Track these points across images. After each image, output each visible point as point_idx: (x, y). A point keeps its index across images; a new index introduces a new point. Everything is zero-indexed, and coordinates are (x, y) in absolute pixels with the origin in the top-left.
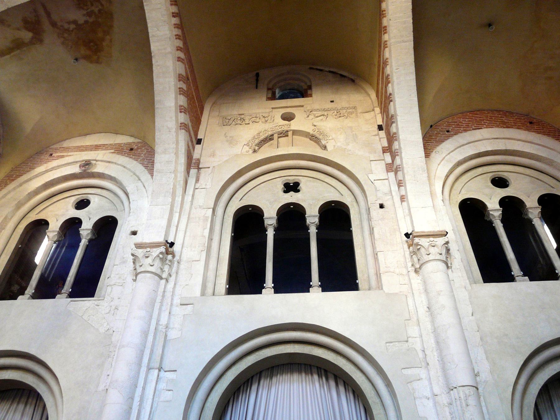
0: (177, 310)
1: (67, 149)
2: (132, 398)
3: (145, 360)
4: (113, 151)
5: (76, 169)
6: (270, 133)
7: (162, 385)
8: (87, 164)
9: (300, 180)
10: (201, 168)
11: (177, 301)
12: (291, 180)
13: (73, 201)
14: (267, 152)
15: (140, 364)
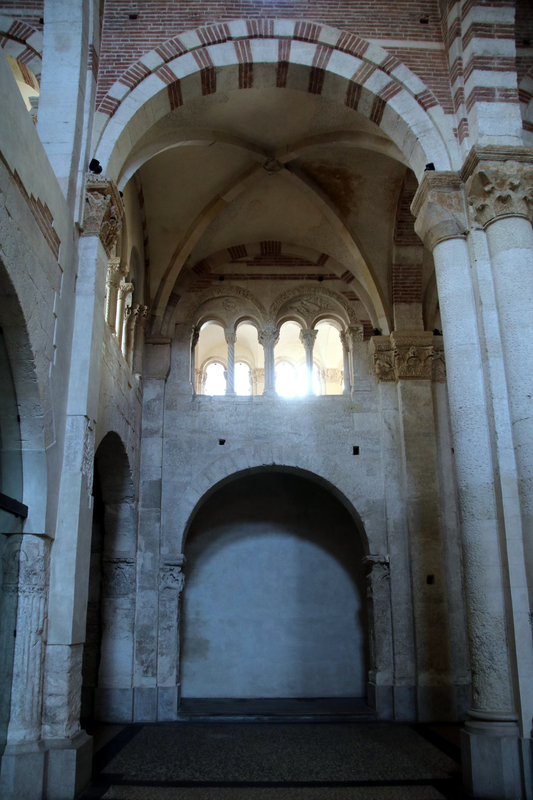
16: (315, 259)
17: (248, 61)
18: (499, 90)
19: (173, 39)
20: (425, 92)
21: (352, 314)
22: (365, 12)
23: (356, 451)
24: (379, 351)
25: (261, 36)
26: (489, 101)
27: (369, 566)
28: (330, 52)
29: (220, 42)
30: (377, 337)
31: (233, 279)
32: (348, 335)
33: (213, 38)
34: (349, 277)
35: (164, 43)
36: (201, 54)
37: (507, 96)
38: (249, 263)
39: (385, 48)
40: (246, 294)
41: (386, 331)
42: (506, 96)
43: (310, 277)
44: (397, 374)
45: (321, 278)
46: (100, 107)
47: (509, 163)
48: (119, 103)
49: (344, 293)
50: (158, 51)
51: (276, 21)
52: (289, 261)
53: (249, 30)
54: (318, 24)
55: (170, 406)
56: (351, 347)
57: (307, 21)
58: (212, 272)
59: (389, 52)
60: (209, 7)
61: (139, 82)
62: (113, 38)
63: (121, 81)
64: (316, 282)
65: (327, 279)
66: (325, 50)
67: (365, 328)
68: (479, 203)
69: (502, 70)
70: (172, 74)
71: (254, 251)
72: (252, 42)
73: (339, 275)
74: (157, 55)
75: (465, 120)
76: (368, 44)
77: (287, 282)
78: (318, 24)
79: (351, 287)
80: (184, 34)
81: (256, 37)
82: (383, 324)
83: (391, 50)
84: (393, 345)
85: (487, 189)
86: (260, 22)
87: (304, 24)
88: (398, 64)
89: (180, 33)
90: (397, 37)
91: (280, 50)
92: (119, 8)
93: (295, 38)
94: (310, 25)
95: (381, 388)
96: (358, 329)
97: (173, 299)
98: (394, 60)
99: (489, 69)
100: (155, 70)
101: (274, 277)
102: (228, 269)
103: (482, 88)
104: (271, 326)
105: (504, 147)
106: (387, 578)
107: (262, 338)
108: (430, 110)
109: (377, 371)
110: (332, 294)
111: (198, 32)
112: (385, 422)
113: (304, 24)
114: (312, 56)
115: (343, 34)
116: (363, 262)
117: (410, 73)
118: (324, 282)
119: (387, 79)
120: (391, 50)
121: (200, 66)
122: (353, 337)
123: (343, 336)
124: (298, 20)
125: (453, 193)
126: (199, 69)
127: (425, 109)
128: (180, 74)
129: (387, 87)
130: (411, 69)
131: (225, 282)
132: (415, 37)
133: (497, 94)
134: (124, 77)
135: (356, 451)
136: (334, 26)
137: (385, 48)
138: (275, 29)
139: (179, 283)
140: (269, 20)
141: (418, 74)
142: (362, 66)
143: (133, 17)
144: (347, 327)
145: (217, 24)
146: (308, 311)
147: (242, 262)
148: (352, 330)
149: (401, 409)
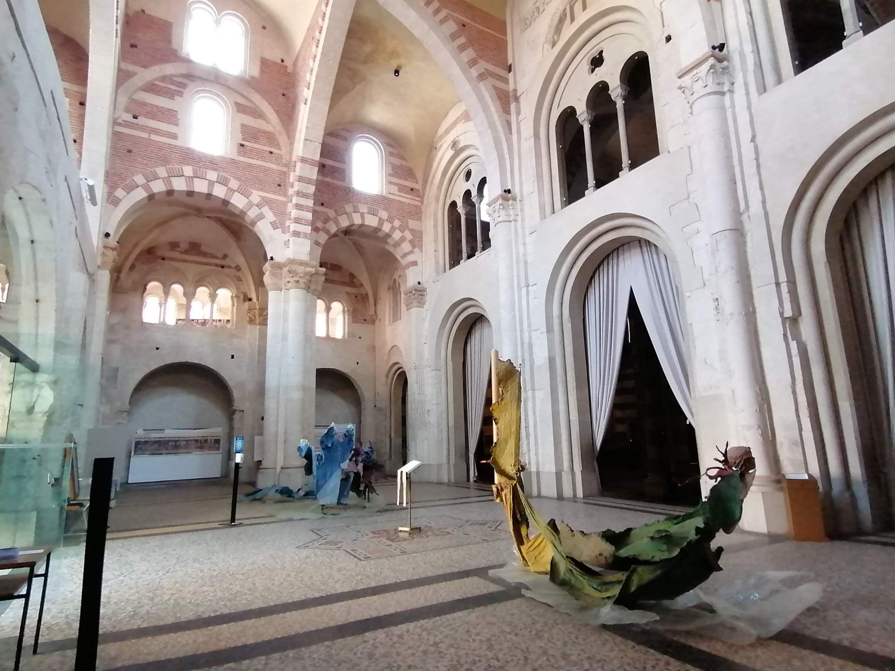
0: (529, 239)
1: (441, 137)
2: (514, 311)
3: (516, 285)
4: (463, 121)
5: (451, 153)
6: (562, 9)
7: (531, 297)
8: (454, 144)
9: (601, 48)
10: (520, 96)
11: (527, 232)
12: (595, 53)
13: (462, 176)
14: (569, 30)
15: (512, 287)
16: (220, 255)
17: (192, 190)
19: (152, 170)
20: (275, 221)
21: (238, 289)
23: (233, 357)
24: (250, 309)
25: (200, 178)
27: (234, 412)
28: (233, 193)
29: (178, 176)
30: (250, 302)
32: (234, 298)
33: (174, 174)
34: (238, 268)
35: (147, 171)
36: (167, 181)
37: (306, 236)
38: (181, 253)
39: (259, 196)
40: (177, 270)
41: (255, 300)
42: (305, 236)
43: (217, 265)
44: (258, 322)
45: (223, 267)
46: (110, 201)
47: (300, 267)
48: (121, 200)
49: (235, 276)
50: (143, 174)
51: (208, 171)
52: (205, 254)
53: (194, 174)
54: (229, 177)
55: (127, 327)
56: (236, 305)
57: (224, 174)
60: (173, 156)
61: (132, 190)
62: (117, 162)
63: (122, 188)
64: (220, 268)
65: (226, 267)
66: (231, 191)
67: (244, 296)
68: (288, 279)
70: (151, 189)
71: (184, 246)
72: (195, 179)
73: (233, 266)
74: (143, 178)
75: (289, 240)
76: (252, 193)
78: (229, 177)
79: (239, 274)
80: (158, 168)
81: (197, 177)
82: (253, 296)
84: (257, 308)
85: (291, 275)
86: (200, 170)
87: (222, 175)
88: (264, 206)
89: (157, 167)
90: (266, 191)
91: (208, 187)
92: (121, 144)
93: (217, 182)
94: (225, 177)
95: (249, 327)
96: (240, 297)
97: (132, 267)
98: (263, 203)
100: (141, 186)
103: (296, 231)
104: (191, 289)
105: (299, 260)
106: (242, 417)
107: (185, 294)
108: (276, 230)
109: (248, 319)
110: (228, 276)
111: (166, 169)
112: (250, 344)
113: (222, 175)
114: (225, 193)
116: (246, 265)
118: (224, 269)
119: (258, 211)
120: (263, 198)
121: (167, 188)
122: (237, 300)
123: (232, 297)
125: (279, 271)
126: (165, 189)
127: (274, 229)
128: (155, 190)
129: (258, 215)
130: (270, 209)
131: (166, 262)
132: (274, 193)
133: (302, 234)
134: (124, 186)
135: (233, 357)
137: (259, 196)
138: (207, 175)
139: (137, 259)
140: (205, 170)
142: (248, 202)
143: (129, 151)
144: (234, 295)
145: (177, 166)
146: (214, 283)
148: (237, 296)
149: (257, 339)
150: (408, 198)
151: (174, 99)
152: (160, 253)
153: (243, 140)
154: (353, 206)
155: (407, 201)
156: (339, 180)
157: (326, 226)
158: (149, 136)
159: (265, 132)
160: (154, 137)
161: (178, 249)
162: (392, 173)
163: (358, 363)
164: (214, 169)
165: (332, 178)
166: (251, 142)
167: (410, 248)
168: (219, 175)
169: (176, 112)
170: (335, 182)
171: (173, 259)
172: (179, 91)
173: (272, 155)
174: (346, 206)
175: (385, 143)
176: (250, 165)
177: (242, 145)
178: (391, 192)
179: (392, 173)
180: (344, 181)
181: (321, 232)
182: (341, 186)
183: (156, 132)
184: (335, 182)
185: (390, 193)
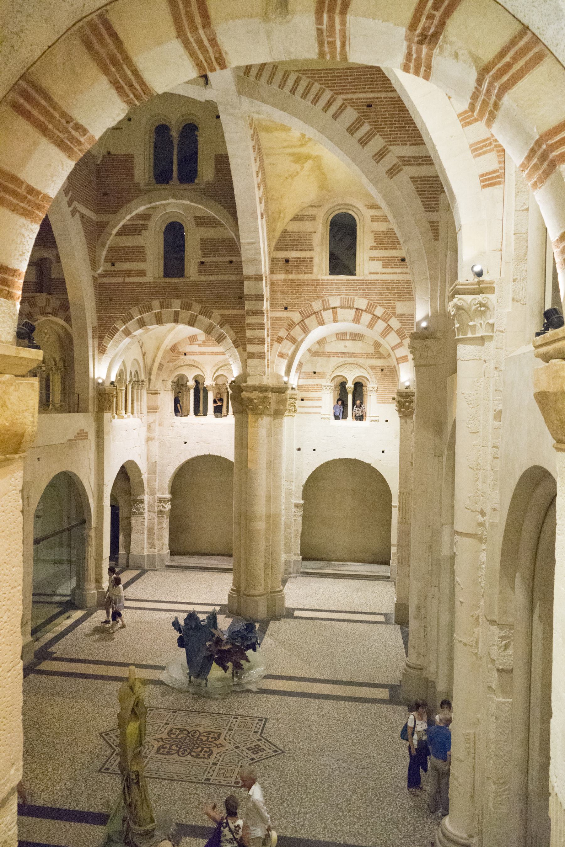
18: (257, 353)
22: (213, 293)
26: (252, 358)
31: (191, 355)
38: (199, 345)
39: (220, 315)
51: (172, 300)
57: (186, 300)
58: (180, 350)
59: (223, 317)
69: (259, 344)
77: (219, 356)
78: (191, 302)
83: (222, 316)
97: (161, 367)
99: (254, 344)
101: (212, 353)
102: (188, 349)
115: (202, 307)
117: (230, 329)
120: (222, 316)
124: (182, 300)
130: (231, 327)
136: (198, 302)
137: (220, 315)
141: (233, 330)
147: (196, 344)
150: (396, 273)
151: (141, 235)
152: (182, 350)
153: (203, 257)
154: (323, 301)
155: (395, 277)
156: (305, 273)
157: (292, 333)
158: (124, 280)
159: (224, 241)
160: (128, 280)
161: (197, 343)
162: (374, 244)
163: (383, 452)
164: (178, 297)
165: (296, 273)
166: (209, 257)
167: (399, 341)
168: (182, 302)
169: (143, 247)
170: (302, 277)
171: (193, 353)
172: (145, 225)
173: (231, 265)
174: (313, 304)
175: (366, 205)
176: (211, 283)
177: (202, 263)
178: (372, 271)
179: (374, 244)
180: (311, 273)
181: (285, 341)
182: (307, 280)
183: (129, 273)
184: (302, 277)
185: (370, 273)
